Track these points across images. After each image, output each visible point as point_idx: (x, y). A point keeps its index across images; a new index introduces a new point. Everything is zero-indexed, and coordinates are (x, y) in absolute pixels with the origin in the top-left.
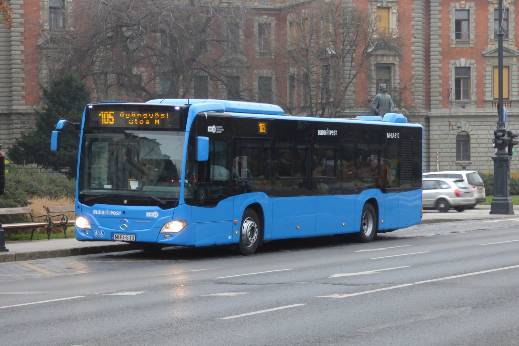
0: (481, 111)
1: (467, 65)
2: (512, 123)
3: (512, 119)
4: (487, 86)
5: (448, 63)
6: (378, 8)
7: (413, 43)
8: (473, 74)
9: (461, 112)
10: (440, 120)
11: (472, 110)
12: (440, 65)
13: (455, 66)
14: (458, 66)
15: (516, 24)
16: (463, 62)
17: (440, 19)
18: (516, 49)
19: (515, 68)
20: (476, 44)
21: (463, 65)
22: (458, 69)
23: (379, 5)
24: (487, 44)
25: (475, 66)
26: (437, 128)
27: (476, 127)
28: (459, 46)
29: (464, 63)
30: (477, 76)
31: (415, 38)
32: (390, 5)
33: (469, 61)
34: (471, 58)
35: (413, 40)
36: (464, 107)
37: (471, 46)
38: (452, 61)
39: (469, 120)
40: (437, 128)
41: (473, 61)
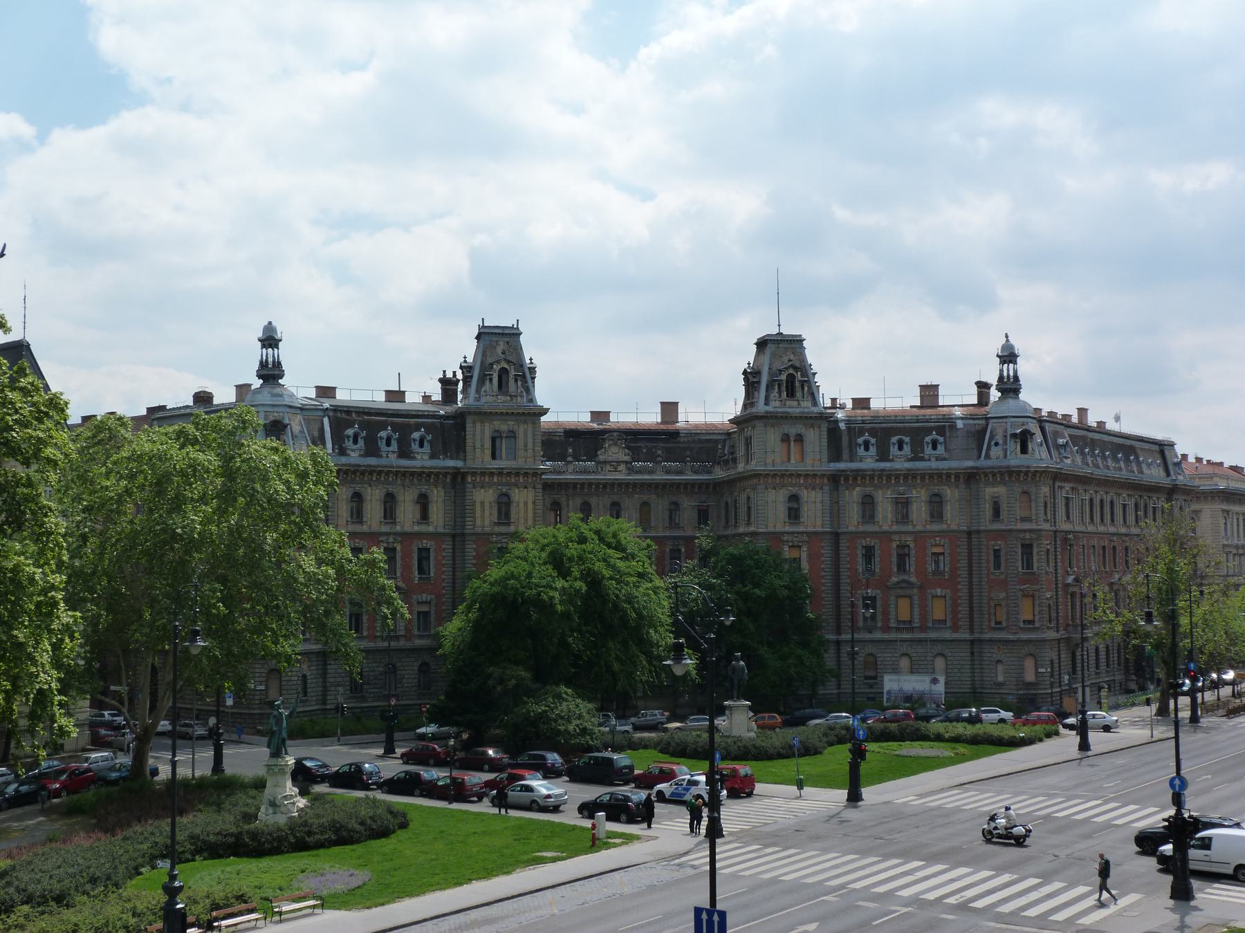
0: (886, 636)
9: (868, 636)
11: (877, 635)
19: (916, 598)
24: (890, 577)
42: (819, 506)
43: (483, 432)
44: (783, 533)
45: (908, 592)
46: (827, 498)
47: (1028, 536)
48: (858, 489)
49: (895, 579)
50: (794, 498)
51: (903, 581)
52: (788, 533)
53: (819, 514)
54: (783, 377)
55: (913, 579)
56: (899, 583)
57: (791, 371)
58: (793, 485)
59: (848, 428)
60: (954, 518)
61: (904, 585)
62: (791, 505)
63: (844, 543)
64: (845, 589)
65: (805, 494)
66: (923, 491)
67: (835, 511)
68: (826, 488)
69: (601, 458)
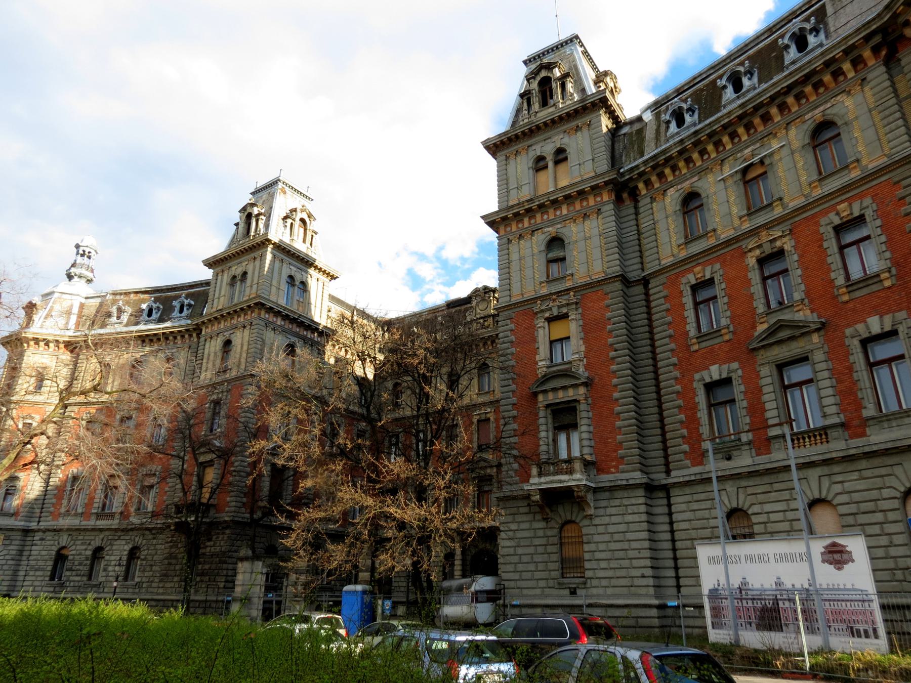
0: (763, 461)
1: (724, 375)
2: (839, 478)
3: (836, 469)
4: (768, 406)
5: (692, 380)
6: (550, 320)
7: (613, 358)
8: (738, 389)
10: (687, 490)
12: (678, 388)
14: (708, 380)
15: (805, 269)
16: (715, 372)
17: (667, 310)
18: (813, 317)
20: (734, 333)
21: (716, 377)
22: (710, 387)
23: (547, 315)
24: (754, 327)
25: (740, 372)
26: (683, 507)
27: (761, 497)
29: (718, 373)
30: (745, 393)
31: (616, 350)
32: (564, 310)
33: (725, 367)
36: (729, 458)
37: (727, 337)
38: (697, 376)
39: (744, 483)
40: (683, 507)
41: (735, 365)
42: (596, 241)
43: (222, 281)
44: (534, 300)
48: (671, 192)
49: (761, 328)
50: (556, 242)
51: (780, 326)
52: (543, 298)
53: (597, 253)
54: (535, 85)
55: (804, 315)
57: (544, 74)
58: (552, 223)
59: (657, 116)
62: (551, 255)
63: (657, 288)
64: (669, 376)
65: (573, 232)
66: (793, 132)
67: (631, 242)
68: (609, 209)
69: (468, 319)
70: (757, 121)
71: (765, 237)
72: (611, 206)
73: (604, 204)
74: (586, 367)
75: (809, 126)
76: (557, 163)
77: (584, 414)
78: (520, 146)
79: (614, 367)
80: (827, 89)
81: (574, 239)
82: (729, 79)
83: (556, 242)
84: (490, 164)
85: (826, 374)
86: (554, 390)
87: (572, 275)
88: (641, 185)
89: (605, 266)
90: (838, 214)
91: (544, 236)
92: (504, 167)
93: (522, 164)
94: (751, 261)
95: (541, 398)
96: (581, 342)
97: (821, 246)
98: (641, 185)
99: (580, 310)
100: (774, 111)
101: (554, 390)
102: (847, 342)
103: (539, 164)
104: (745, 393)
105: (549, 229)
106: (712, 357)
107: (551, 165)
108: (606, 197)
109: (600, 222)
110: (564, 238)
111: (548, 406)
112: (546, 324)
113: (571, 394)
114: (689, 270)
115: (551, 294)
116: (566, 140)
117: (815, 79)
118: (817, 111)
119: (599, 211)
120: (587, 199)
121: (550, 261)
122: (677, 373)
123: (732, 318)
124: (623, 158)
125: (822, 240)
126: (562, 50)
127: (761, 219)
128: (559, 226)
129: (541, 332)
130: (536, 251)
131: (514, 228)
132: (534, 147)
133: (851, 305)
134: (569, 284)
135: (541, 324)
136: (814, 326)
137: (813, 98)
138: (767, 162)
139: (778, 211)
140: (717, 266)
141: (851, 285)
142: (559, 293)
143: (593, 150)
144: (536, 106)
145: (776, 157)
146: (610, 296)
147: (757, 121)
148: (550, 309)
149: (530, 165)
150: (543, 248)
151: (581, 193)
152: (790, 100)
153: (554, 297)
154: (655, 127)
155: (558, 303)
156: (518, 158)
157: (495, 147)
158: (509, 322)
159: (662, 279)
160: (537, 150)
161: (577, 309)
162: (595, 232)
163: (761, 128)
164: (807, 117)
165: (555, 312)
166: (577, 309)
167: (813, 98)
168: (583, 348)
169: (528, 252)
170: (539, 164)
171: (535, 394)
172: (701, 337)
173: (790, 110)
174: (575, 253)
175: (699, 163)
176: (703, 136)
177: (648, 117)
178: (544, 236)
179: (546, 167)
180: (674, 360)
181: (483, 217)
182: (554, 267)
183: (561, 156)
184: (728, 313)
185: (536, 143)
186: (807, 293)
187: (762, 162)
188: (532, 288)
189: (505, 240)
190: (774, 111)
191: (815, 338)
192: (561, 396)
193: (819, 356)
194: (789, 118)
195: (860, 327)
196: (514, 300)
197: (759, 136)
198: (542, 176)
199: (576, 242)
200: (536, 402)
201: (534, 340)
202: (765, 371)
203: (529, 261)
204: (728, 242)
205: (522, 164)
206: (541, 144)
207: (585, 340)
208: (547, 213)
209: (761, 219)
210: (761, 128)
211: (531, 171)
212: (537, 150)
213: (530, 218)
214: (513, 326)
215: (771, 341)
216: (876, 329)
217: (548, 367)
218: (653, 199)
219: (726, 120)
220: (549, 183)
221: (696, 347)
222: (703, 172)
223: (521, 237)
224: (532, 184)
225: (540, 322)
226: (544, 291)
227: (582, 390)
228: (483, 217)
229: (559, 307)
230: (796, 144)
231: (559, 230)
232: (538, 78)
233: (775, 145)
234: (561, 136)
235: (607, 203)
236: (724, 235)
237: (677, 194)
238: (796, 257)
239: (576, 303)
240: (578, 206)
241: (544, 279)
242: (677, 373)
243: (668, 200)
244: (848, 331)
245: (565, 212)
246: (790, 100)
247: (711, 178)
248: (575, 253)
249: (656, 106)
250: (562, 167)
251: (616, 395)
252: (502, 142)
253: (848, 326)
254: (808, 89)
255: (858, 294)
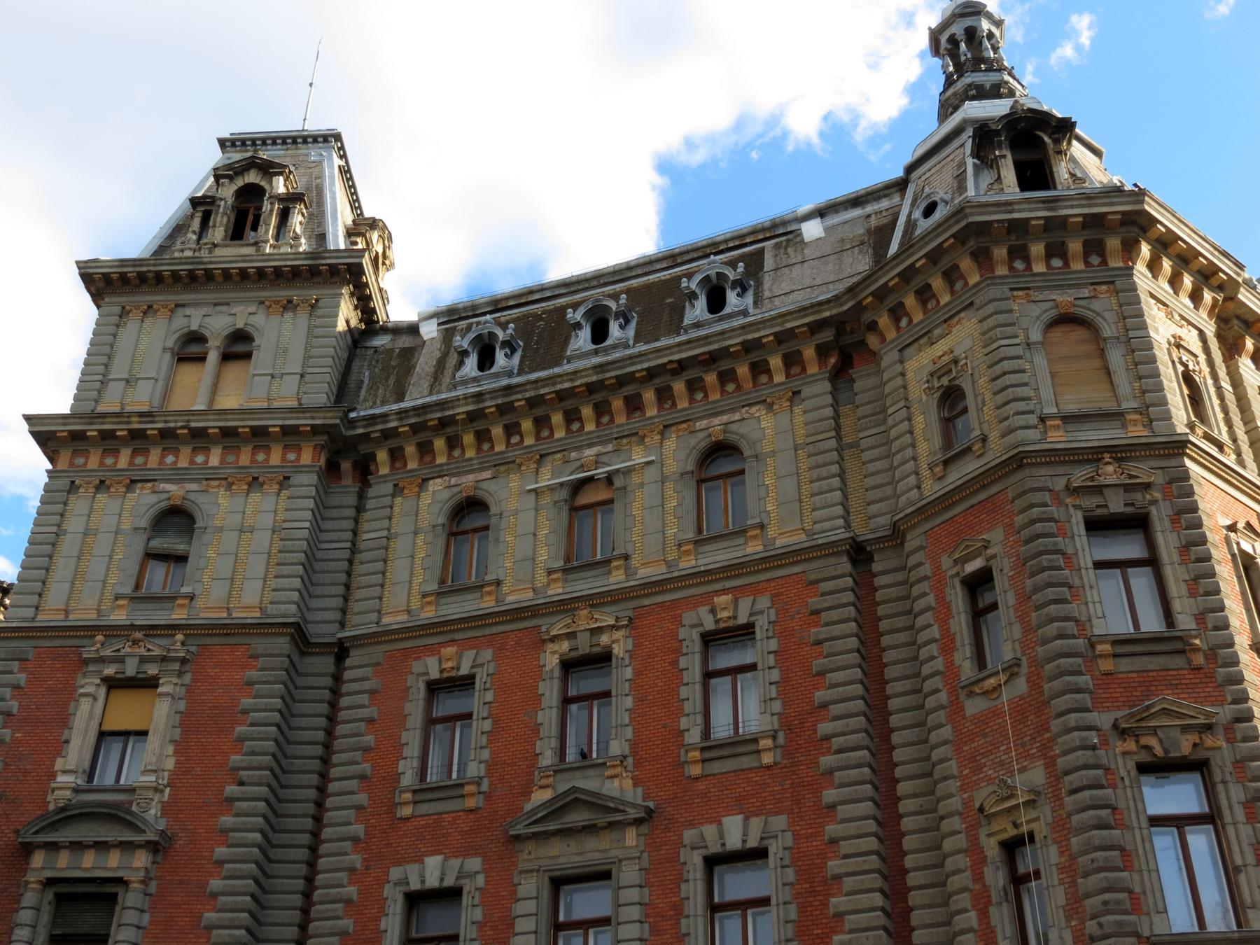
1: (449, 882)
5: (382, 881)
6: (113, 684)
7: (231, 800)
12: (352, 891)
13: (404, 889)
14: (415, 885)
15: (640, 700)
16: (433, 871)
17: (370, 721)
20: (488, 796)
21: (432, 882)
22: (415, 900)
23: (110, 671)
24: (527, 793)
25: (480, 880)
28: (425, 808)
29: (437, 873)
30: (481, 925)
31: (241, 783)
32: (152, 670)
33: (455, 863)
34: (466, 851)
35: (231, 789)
37: (471, 803)
41: (474, 864)
42: (263, 539)
44: (90, 630)
45: (589, 852)
46: (302, 513)
47: (1110, 473)
48: (435, 485)
49: (541, 796)
50: (176, 517)
52: (113, 632)
53: (257, 566)
54: (228, 192)
55: (619, 787)
56: (558, 808)
57: (252, 177)
58: (180, 476)
59: (447, 336)
60: (786, 499)
61: (578, 817)
62: (159, 544)
64: (339, 859)
65: (220, 508)
66: (671, 444)
67: (334, 560)
68: (307, 482)
70: (617, 404)
71: (583, 619)
72: (313, 478)
73: (299, 469)
74: (166, 809)
75: (699, 442)
76: (227, 358)
77: (130, 917)
78: (157, 298)
79: (227, 820)
80: (739, 388)
81: (217, 523)
82: (587, 314)
83: (176, 517)
84: (79, 314)
85: (635, 912)
86: (77, 846)
87: (192, 597)
88: (382, 456)
89: (269, 597)
90: (713, 611)
91: (153, 499)
92: (112, 329)
93: (152, 338)
94: (551, 660)
95: (38, 859)
96: (170, 749)
97: (675, 663)
98: (382, 456)
99: (187, 679)
100: (649, 396)
101: (77, 846)
102: (684, 855)
103: (189, 349)
104: (481, 925)
105: (169, 487)
106: (433, 838)
107: (213, 357)
108: (306, 457)
109: (282, 503)
110: (197, 515)
111: (50, 882)
112: (103, 690)
113: (113, 863)
114: (433, 650)
115: (133, 627)
116: (259, 319)
117: (724, 365)
118: (716, 421)
119: (285, 481)
120: (267, 449)
121: (152, 556)
122: (356, 860)
123: (491, 766)
124: (363, 392)
125: (678, 652)
126: (303, 150)
127: (586, 585)
128: (194, 486)
129: (85, 705)
130: (126, 525)
131: (93, 463)
132: (188, 311)
133: (701, 786)
134: (178, 615)
135: (90, 689)
136: (633, 813)
137: (715, 396)
138: (618, 482)
139: (616, 579)
140: (487, 654)
141: (711, 749)
142: (152, 630)
143: (307, 357)
144: (218, 233)
145: (635, 479)
146: (261, 662)
147: (617, 404)
148: (121, 660)
149: (170, 343)
150: (144, 522)
151: (259, 435)
152: (679, 386)
153: (138, 635)
154: (438, 354)
155: (142, 651)
156: (149, 321)
157: (103, 281)
158: (15, 665)
159: (377, 653)
160: (194, 318)
161: (180, 674)
162: (267, 520)
163: (621, 419)
164: (699, 425)
165: (131, 669)
166: (180, 674)
167: (715, 396)
168: (170, 764)
169: (108, 523)
170: (189, 349)
171: (27, 849)
172: (423, 792)
173: (674, 404)
174: (211, 553)
175: (500, 447)
176: (519, 400)
177: (430, 331)
178: (153, 499)
179: (202, 359)
180: (359, 829)
181: (28, 418)
182: (158, 574)
183: (239, 347)
184: (486, 754)
185: (195, 305)
186: (635, 745)
187: (609, 480)
188: (91, 602)
189: (65, 483)
190: (649, 396)
191: (631, 837)
192: (90, 865)
193: (629, 874)
194: (670, 417)
195: (709, 830)
196: (43, 619)
197: (615, 432)
198: (188, 373)
199: (221, 529)
200: (24, 869)
201: (64, 721)
202: (529, 886)
203: (103, 543)
204: (518, 613)
205: (152, 338)
206: (205, 310)
207: (181, 747)
208: (176, 452)
209: (586, 585)
210: (621, 419)
211: (168, 356)
212: (194, 318)
213: (135, 452)
214: (22, 678)
215: (552, 826)
216: (734, 841)
217: (77, 790)
218: (398, 490)
219: (567, 385)
220: (193, 392)
221: (407, 811)
222: (503, 466)
223: (102, 486)
224: (161, 384)
225: (90, 685)
226: (120, 616)
227: (141, 859)
228: (28, 418)
229: (143, 660)
230: (672, 467)
231: (192, 496)
232: (240, 182)
233: (638, 457)
234: (252, 309)
235: (307, 469)
236: (516, 596)
237: (446, 494)
238: (629, 673)
239: (184, 661)
240: (245, 458)
241: (128, 590)
242: (356, 860)
243: (426, 499)
244: (689, 835)
245: (214, 460)
246: (679, 386)
247: (514, 481)
248: (211, 553)
249: (451, 317)
250: (234, 371)
251: (215, 884)
252: (123, 278)
253: (691, 825)
254: (711, 378)
255: (717, 767)
